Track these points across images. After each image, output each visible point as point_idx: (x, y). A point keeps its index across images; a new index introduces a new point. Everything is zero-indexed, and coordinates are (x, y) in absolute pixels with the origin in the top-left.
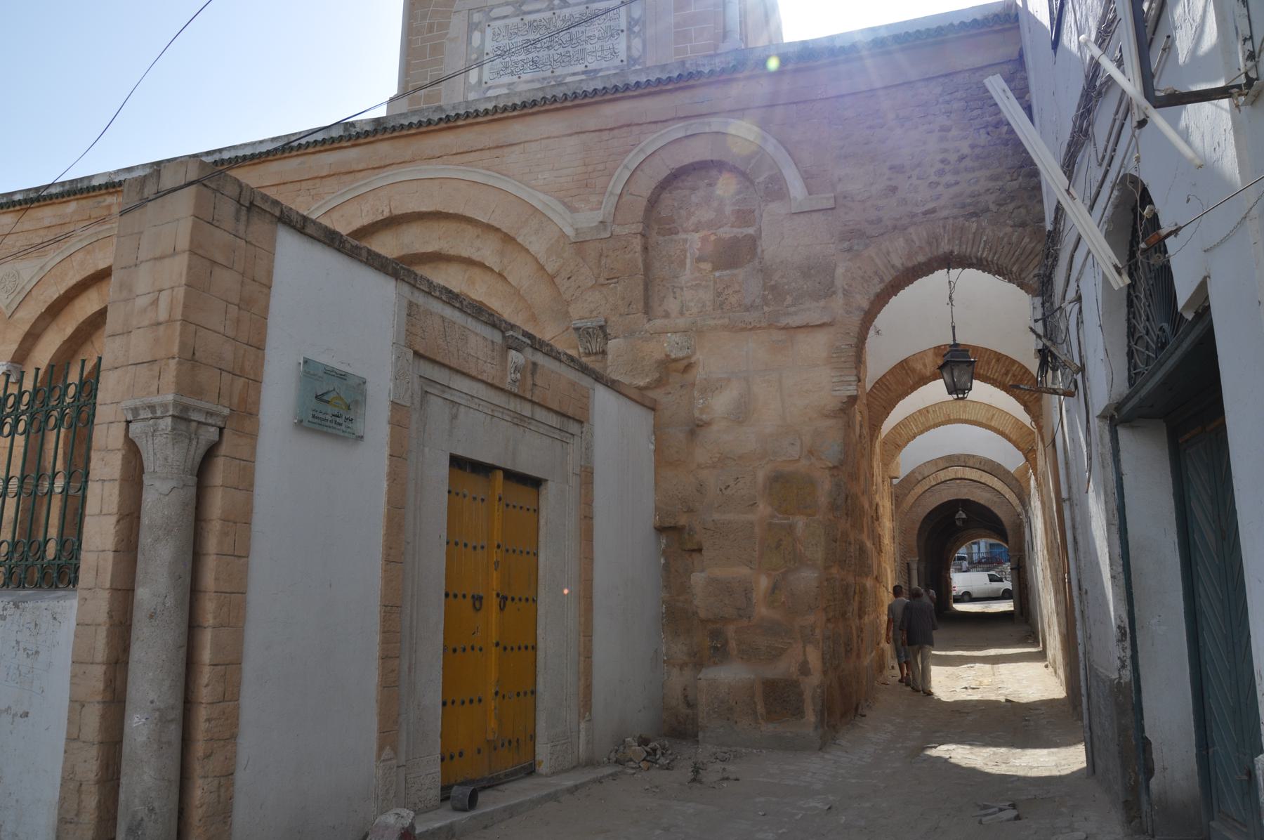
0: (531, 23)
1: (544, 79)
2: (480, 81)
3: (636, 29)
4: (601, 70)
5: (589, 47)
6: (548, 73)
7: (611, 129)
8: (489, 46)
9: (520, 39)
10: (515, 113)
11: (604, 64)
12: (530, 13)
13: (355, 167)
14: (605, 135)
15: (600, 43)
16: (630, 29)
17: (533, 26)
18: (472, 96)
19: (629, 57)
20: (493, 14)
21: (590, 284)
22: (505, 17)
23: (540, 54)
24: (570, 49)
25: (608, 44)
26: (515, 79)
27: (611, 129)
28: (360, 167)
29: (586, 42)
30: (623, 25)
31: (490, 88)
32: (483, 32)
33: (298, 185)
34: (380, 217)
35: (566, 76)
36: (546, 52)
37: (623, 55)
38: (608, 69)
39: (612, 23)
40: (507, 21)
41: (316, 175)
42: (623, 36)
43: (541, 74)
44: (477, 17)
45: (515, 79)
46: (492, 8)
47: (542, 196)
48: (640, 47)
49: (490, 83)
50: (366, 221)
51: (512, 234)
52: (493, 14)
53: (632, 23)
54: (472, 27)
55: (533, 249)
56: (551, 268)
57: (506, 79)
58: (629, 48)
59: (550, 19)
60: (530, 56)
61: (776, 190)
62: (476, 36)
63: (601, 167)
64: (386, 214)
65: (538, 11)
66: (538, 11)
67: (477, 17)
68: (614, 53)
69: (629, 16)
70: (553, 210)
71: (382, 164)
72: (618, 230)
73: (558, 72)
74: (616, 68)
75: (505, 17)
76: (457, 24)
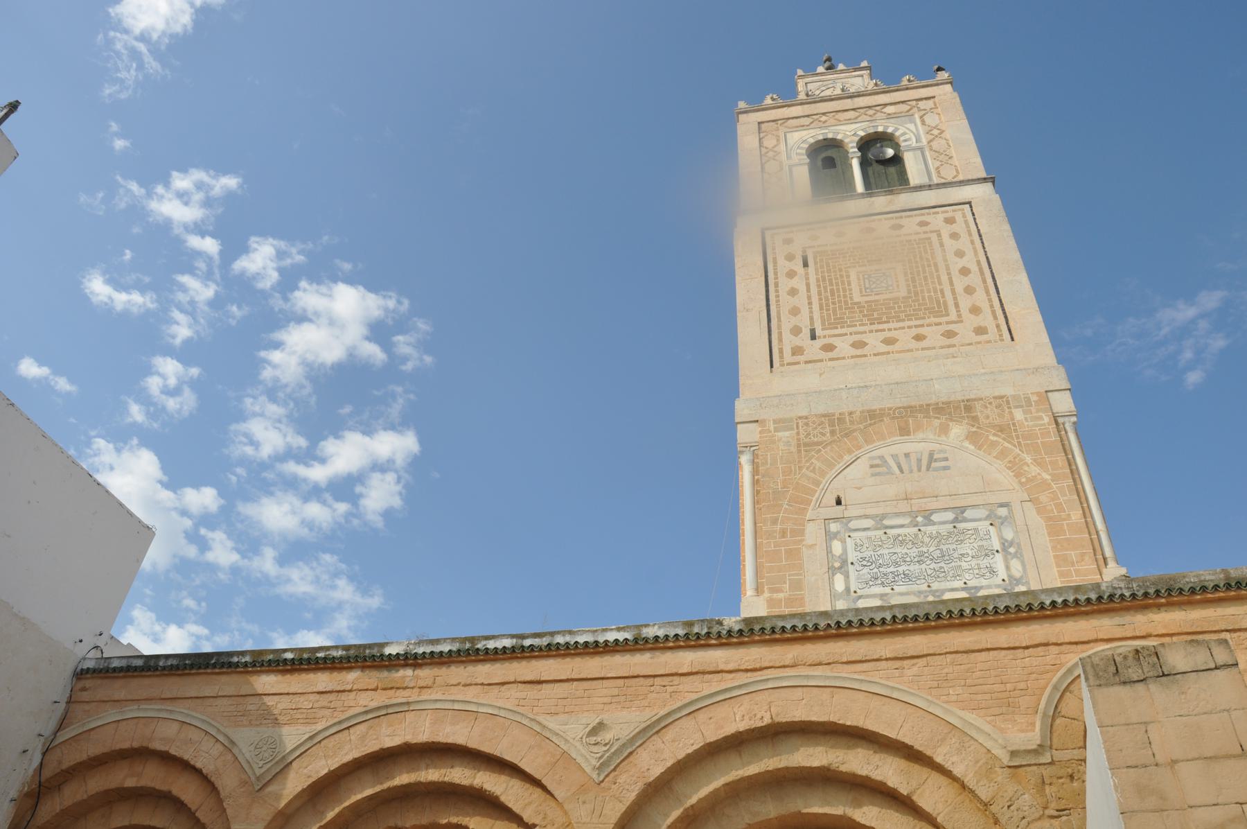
0: (896, 537)
1: (920, 592)
2: (847, 589)
3: (1012, 550)
4: (981, 588)
5: (964, 564)
6: (924, 587)
7: (1027, 648)
8: (852, 556)
9: (887, 551)
10: (916, 625)
11: (984, 582)
12: (892, 527)
13: (721, 667)
14: (1019, 653)
15: (974, 563)
16: (1005, 549)
18: (841, 605)
19: (1010, 577)
20: (853, 525)
21: (1037, 815)
22: (865, 529)
23: (911, 568)
24: (942, 564)
25: (985, 562)
26: (888, 590)
27: (1027, 648)
28: (730, 667)
29: (960, 559)
30: (997, 545)
31: (860, 597)
32: (843, 542)
33: (650, 681)
34: (760, 724)
35: (943, 591)
36: (917, 566)
37: (1002, 574)
38: (989, 587)
39: (984, 543)
40: (869, 533)
41: (674, 671)
42: (999, 558)
43: (915, 588)
44: (834, 527)
45: (888, 590)
46: (850, 519)
47: (962, 713)
48: (1020, 568)
49: (860, 592)
50: (742, 726)
51: (928, 752)
52: (853, 525)
53: (1006, 545)
54: (830, 536)
55: (958, 771)
56: (984, 794)
57: (878, 590)
58: (1008, 568)
59: (916, 535)
60: (901, 569)
62: (837, 547)
63: (1022, 685)
64: (767, 721)
65: (902, 526)
66: (902, 526)
67: (834, 527)
68: (993, 572)
69: (1001, 538)
70: (978, 729)
71: (758, 666)
72: (1058, 755)
73: (935, 586)
74: (998, 586)
75: (865, 529)
76: (813, 533)
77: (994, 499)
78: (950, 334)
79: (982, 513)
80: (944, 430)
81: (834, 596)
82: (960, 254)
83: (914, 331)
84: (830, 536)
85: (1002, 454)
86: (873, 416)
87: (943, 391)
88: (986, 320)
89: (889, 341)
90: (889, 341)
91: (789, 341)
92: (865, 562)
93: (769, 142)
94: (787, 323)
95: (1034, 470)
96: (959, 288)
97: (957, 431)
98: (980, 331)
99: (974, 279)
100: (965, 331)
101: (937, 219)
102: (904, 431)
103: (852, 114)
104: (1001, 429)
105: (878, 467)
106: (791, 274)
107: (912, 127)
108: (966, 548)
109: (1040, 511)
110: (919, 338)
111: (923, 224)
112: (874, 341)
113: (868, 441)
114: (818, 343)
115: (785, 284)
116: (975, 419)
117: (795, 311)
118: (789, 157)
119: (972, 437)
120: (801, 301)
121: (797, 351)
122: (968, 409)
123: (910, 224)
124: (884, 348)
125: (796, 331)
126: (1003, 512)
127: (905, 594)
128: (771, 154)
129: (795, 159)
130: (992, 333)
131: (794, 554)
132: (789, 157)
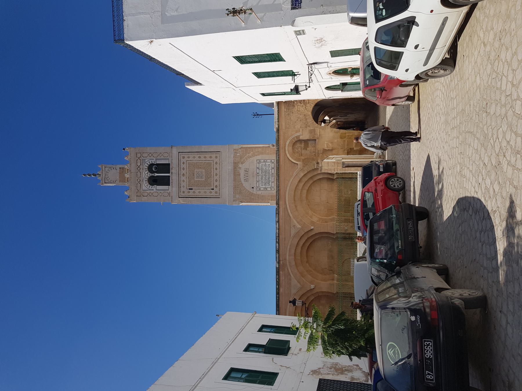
17: (262, 178)
54: (260, 190)
61: (298, 137)
76: (259, 192)
77: (256, 162)
78: (216, 163)
79: (258, 165)
80: (240, 168)
81: (271, 190)
82: (194, 157)
83: (215, 169)
84: (260, 190)
85: (246, 159)
86: (235, 180)
87: (230, 167)
88: (214, 156)
89: (216, 175)
90: (216, 175)
91: (213, 193)
92: (265, 184)
93: (146, 194)
94: (208, 194)
95: (250, 155)
96: (205, 159)
97: (240, 166)
98: (216, 157)
99: (202, 156)
100: (217, 160)
101: (183, 160)
102: (240, 175)
103: (139, 173)
104: (241, 158)
105: (246, 180)
106: (194, 192)
107: (146, 160)
108: (264, 168)
109: (259, 155)
110: (216, 169)
111: (184, 163)
112: (215, 178)
113: (241, 181)
114: (215, 188)
115: (197, 193)
116: (238, 162)
117: (205, 192)
118: (153, 190)
119: (242, 163)
120: (202, 191)
121: (216, 192)
122: (236, 163)
123: (182, 166)
124: (218, 176)
125: (211, 192)
126: (258, 161)
127: (273, 179)
128: (150, 194)
129: (155, 189)
130: (218, 155)
131: (263, 196)
132: (153, 190)
